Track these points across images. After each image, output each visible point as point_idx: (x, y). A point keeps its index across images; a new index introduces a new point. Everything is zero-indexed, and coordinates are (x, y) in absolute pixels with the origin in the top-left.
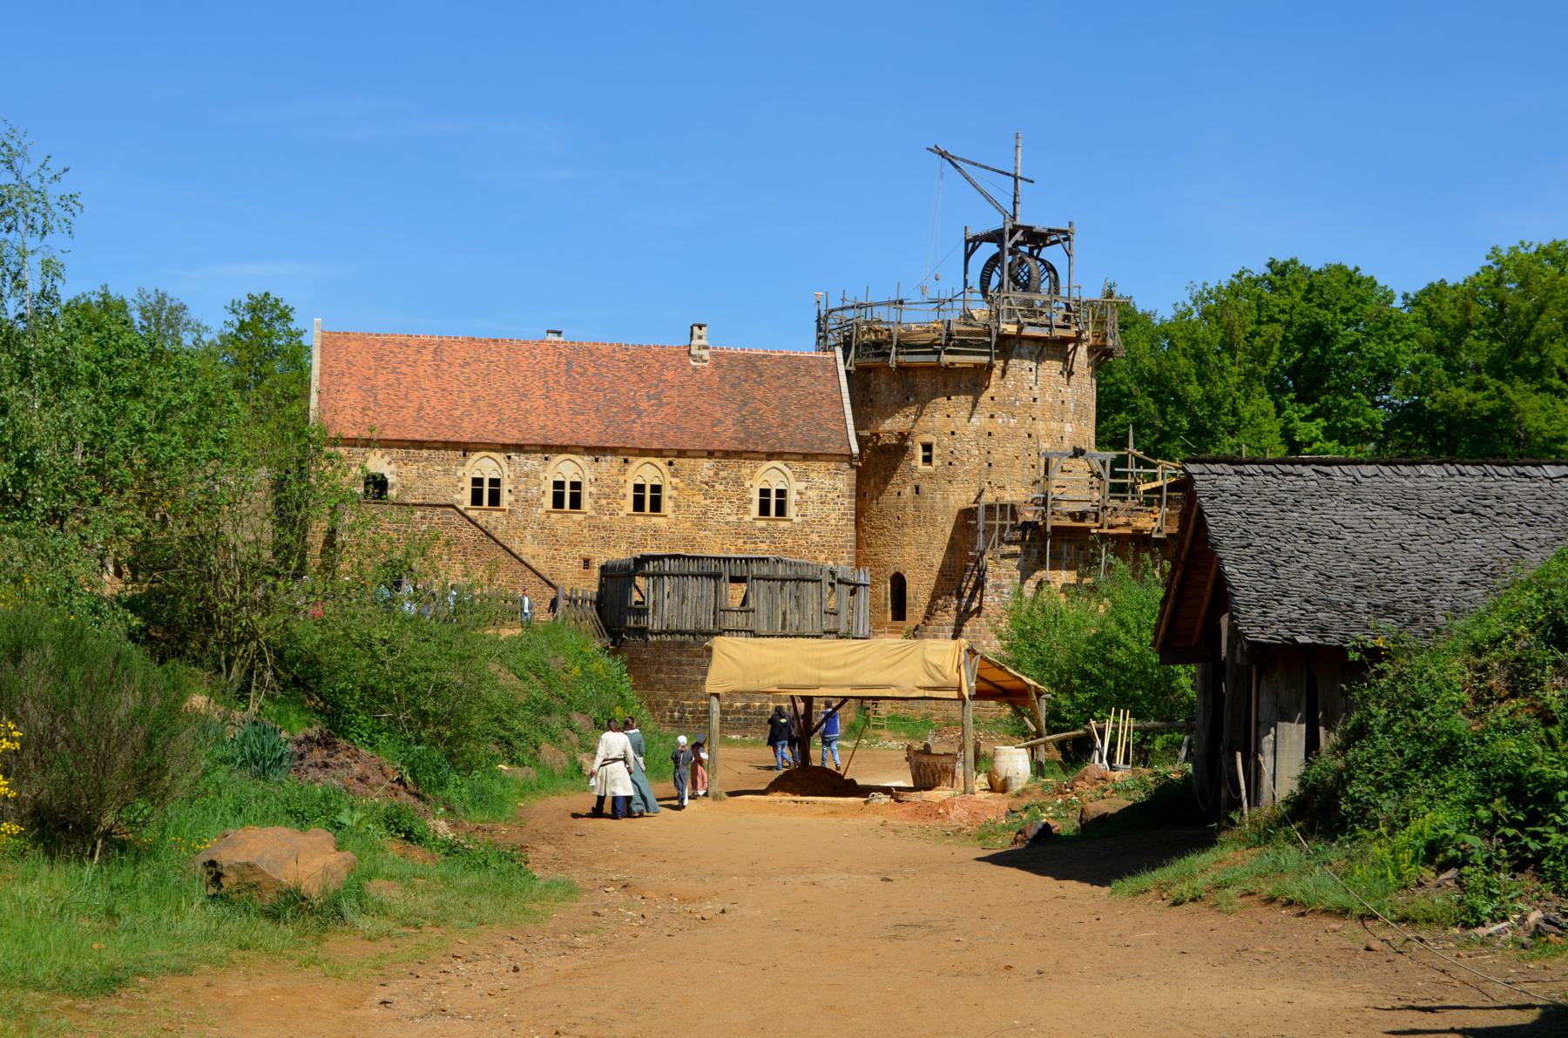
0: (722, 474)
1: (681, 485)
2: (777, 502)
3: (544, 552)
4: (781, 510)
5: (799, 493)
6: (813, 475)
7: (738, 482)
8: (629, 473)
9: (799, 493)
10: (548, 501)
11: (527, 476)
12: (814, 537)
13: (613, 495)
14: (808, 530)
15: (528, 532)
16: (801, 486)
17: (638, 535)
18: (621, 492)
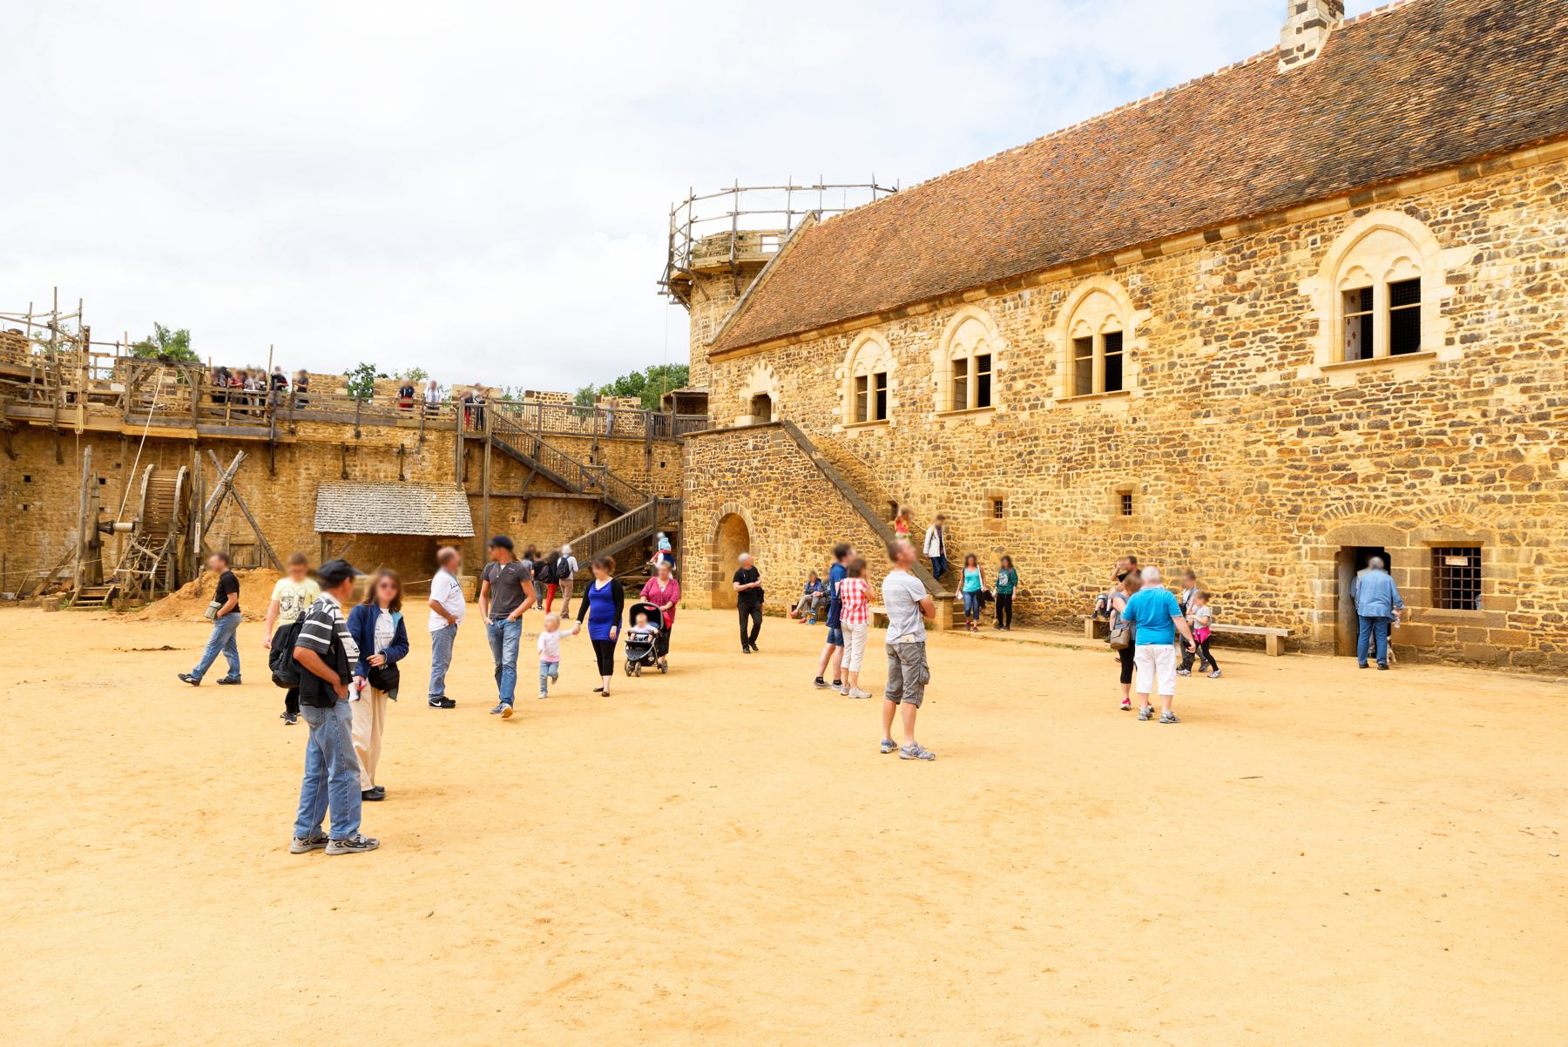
0: (1243, 277)
1: (1156, 323)
2: (1395, 317)
3: (939, 492)
4: (1406, 336)
5: (1455, 279)
6: (1495, 219)
7: (1284, 289)
8: (1061, 320)
9: (1455, 279)
10: (943, 400)
11: (914, 361)
12: (1511, 396)
13: (1033, 367)
14: (1488, 379)
15: (916, 458)
16: (1460, 258)
17: (1077, 442)
18: (1048, 359)
